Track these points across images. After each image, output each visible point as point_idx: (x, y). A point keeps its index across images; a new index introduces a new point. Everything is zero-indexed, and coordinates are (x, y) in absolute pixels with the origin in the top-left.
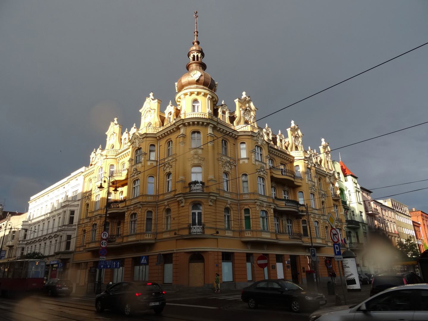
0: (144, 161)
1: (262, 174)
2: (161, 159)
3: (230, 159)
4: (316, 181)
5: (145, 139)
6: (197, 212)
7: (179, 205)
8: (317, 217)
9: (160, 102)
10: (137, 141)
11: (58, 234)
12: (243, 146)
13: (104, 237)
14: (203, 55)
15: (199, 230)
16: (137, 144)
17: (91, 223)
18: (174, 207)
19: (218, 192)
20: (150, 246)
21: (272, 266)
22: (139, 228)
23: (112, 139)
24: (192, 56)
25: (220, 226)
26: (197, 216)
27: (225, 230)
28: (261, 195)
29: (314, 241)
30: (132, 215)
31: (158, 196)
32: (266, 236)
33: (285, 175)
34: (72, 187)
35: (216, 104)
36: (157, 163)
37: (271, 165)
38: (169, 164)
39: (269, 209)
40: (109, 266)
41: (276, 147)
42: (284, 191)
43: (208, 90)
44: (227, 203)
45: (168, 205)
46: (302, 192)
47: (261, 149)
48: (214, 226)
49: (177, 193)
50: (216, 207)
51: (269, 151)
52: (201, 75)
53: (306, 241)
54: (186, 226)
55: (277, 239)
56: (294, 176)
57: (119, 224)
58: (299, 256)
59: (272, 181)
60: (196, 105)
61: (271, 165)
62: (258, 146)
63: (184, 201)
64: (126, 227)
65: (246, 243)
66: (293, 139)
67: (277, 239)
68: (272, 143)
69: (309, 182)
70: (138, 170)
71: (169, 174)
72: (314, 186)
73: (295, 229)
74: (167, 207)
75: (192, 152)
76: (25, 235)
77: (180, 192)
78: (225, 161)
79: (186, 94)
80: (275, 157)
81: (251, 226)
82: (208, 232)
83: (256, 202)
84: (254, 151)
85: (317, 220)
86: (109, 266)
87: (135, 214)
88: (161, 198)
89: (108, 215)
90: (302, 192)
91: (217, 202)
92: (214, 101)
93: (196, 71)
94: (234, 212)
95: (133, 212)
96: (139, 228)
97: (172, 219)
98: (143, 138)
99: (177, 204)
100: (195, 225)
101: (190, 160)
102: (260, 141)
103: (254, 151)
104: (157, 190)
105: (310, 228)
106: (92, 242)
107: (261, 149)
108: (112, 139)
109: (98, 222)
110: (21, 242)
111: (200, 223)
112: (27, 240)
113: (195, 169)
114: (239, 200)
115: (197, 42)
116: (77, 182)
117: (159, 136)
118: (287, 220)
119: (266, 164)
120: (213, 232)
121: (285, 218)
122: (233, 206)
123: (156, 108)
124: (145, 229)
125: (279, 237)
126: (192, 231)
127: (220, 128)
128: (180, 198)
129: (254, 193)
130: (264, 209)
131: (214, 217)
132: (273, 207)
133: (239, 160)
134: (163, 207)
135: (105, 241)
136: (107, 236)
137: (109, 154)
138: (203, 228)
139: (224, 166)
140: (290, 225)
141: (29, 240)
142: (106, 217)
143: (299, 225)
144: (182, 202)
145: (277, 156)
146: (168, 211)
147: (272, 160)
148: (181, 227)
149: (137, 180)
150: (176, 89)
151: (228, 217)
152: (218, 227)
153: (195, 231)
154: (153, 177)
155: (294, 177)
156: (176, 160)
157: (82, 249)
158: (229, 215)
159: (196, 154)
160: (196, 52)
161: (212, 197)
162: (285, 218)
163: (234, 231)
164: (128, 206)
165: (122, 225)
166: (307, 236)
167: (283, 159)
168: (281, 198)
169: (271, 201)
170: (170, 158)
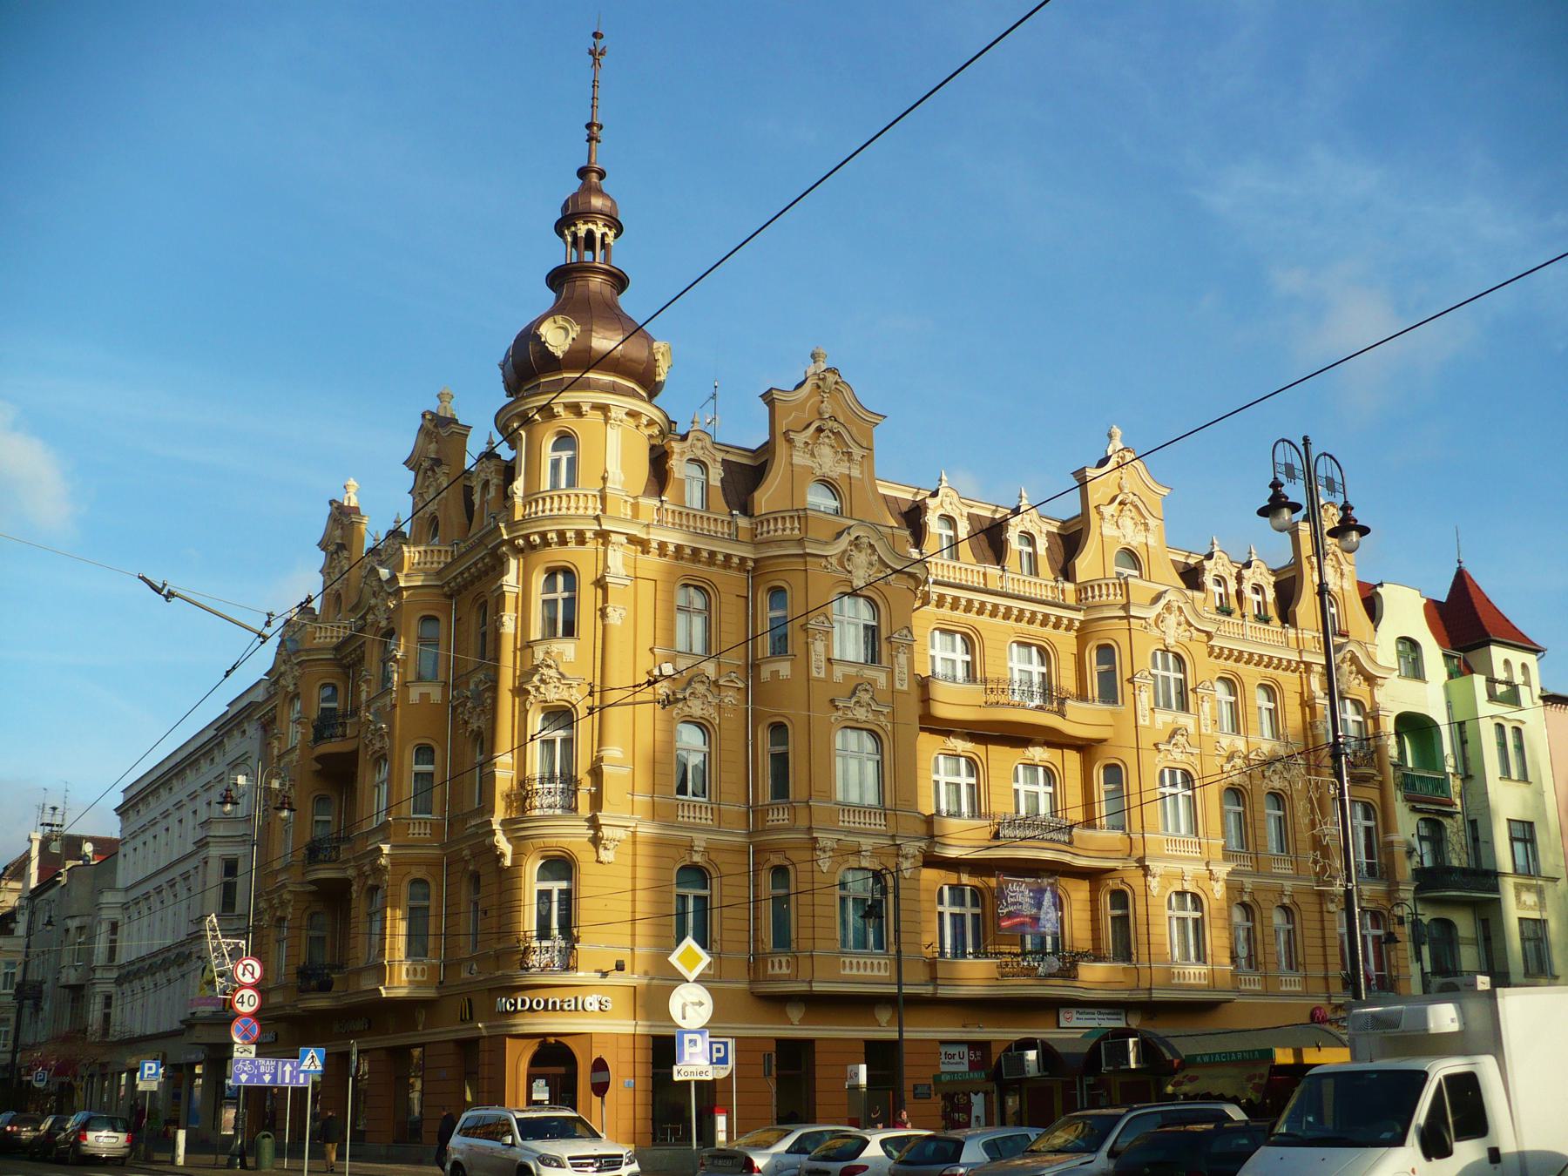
6: (557, 886)
11: (186, 950)
13: (248, 979)
21: (915, 1087)
26: (555, 906)
60: (565, 456)
135: (251, 992)
136: (257, 974)
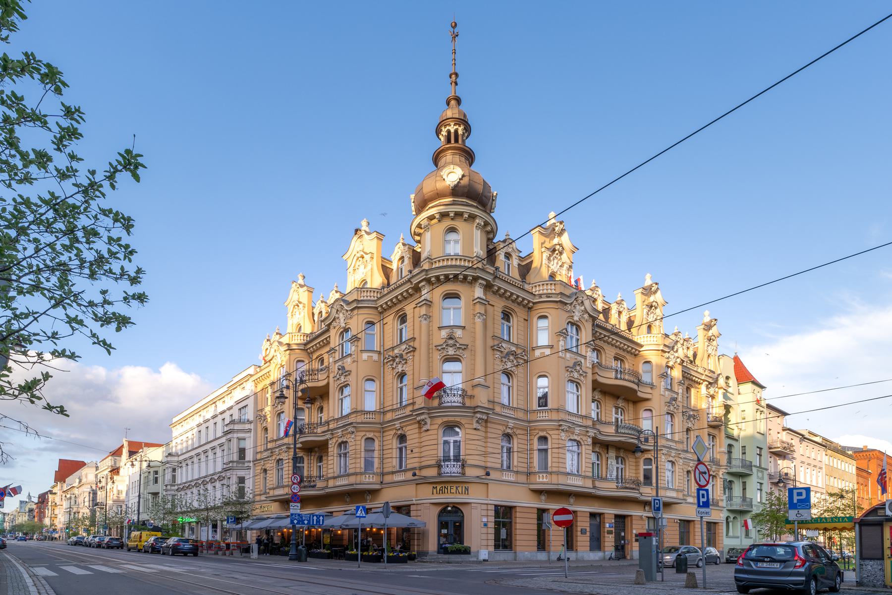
1: (576, 375)
2: (386, 348)
3: (517, 348)
4: (680, 391)
5: (356, 312)
6: (451, 439)
7: (420, 428)
8: (673, 454)
9: (380, 237)
10: (341, 315)
12: (543, 323)
14: (468, 129)
15: (455, 470)
16: (342, 320)
18: (411, 432)
19: (491, 407)
20: (374, 493)
22: (353, 466)
24: (444, 133)
25: (493, 462)
27: (501, 470)
28: (570, 414)
29: (661, 493)
30: (340, 445)
31: (384, 413)
32: (575, 483)
33: (621, 379)
35: (494, 237)
37: (596, 361)
38: (401, 356)
39: (584, 438)
40: (306, 522)
41: (609, 327)
42: (617, 408)
43: (477, 207)
44: (507, 426)
46: (650, 410)
47: (578, 329)
48: (482, 464)
49: (417, 407)
50: (486, 432)
51: (593, 334)
52: (463, 176)
53: (647, 493)
54: (433, 462)
55: (594, 487)
56: (639, 380)
57: (320, 459)
58: (631, 516)
59: (594, 389)
61: (596, 361)
62: (573, 324)
63: (428, 421)
64: (332, 464)
65: (539, 492)
66: (645, 311)
67: (594, 487)
68: (601, 317)
69: (667, 393)
70: (347, 369)
71: (402, 376)
72: (675, 399)
73: (629, 473)
74: (399, 432)
75: (444, 333)
77: (423, 405)
78: (506, 351)
79: (431, 218)
80: (605, 346)
81: (549, 465)
82: (471, 472)
83: (560, 425)
84: (563, 334)
85: (671, 459)
86: (306, 522)
88: (389, 416)
89: (298, 446)
90: (650, 410)
91: (489, 425)
92: (488, 233)
93: (452, 166)
94: (520, 441)
96: (353, 466)
97: (409, 452)
98: (352, 310)
99: (417, 426)
100: (449, 460)
102: (577, 313)
103: (563, 334)
104: (382, 403)
105: (657, 467)
106: (278, 487)
107: (578, 329)
109: (284, 456)
111: (457, 458)
113: (449, 366)
114: (529, 422)
115: (455, 99)
117: (381, 306)
118: (617, 458)
119: (585, 357)
120: (480, 472)
121: (612, 454)
122: (518, 432)
123: (374, 251)
124: (363, 466)
125: (598, 484)
126: (443, 470)
127: (499, 288)
128: (423, 417)
129: (558, 410)
130: (576, 437)
131: (483, 449)
132: (591, 434)
133: (533, 349)
134: (392, 432)
137: (293, 342)
138: (463, 466)
139: (504, 360)
140: (620, 466)
142: (295, 448)
143: (637, 466)
144: (426, 423)
145: (608, 343)
146: (402, 438)
147: (597, 350)
148: (423, 464)
149: (346, 386)
150: (413, 208)
151: (509, 451)
152: (489, 465)
153: (448, 470)
154: (373, 380)
155: (639, 382)
156: (415, 349)
157: (263, 498)
158: (511, 446)
159: (451, 338)
160: (452, 124)
161: (478, 415)
162: (612, 454)
163: (517, 472)
164: (332, 430)
165: (325, 462)
166: (651, 484)
167: (620, 348)
168: (608, 420)
169: (590, 423)
170: (404, 347)
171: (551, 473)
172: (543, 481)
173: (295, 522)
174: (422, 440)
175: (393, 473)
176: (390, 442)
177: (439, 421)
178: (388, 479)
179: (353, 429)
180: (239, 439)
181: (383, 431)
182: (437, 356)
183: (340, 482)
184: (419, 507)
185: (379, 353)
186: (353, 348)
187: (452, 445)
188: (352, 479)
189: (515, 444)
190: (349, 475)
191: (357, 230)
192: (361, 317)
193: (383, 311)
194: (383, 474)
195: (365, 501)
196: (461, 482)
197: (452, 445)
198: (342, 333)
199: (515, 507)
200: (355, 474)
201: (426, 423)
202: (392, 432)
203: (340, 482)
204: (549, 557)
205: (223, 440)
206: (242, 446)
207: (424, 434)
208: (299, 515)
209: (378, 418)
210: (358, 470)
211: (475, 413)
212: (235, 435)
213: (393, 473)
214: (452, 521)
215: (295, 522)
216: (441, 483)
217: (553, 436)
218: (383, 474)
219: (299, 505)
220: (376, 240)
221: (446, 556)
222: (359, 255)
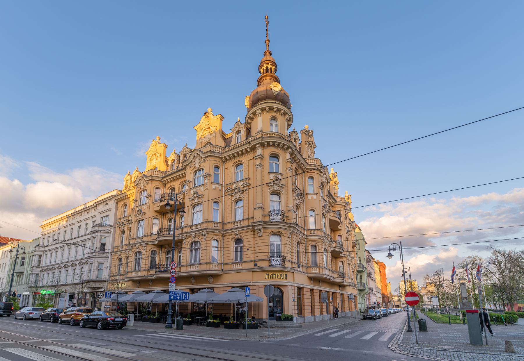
0: (208, 184)
5: (208, 159)
15: (278, 263)
17: (133, 250)
23: (155, 159)
34: (101, 213)
36: (222, 189)
45: (239, 234)
49: (255, 221)
54: (266, 257)
63: (262, 230)
74: (237, 237)
75: (272, 176)
76: (39, 262)
77: (260, 220)
82: (288, 265)
87: (196, 242)
88: (229, 226)
95: (194, 240)
98: (206, 157)
101: (269, 185)
108: (155, 159)
110: (34, 268)
112: (42, 267)
116: (107, 207)
126: (273, 263)
134: (231, 237)
138: (284, 261)
141: (44, 267)
144: (261, 232)
146: (239, 241)
171: (319, 267)
172: (315, 272)
173: (172, 297)
174: (256, 242)
175: (232, 264)
176: (230, 243)
177: (269, 231)
178: (226, 268)
179: (205, 233)
180: (101, 237)
181: (224, 236)
182: (267, 190)
183: (191, 269)
184: (255, 288)
185: (222, 185)
186: (206, 181)
187: (275, 246)
188: (203, 267)
189: (302, 248)
190: (200, 264)
191: (206, 113)
192: (212, 162)
193: (225, 160)
194: (223, 264)
195: (208, 282)
196: (282, 270)
197: (275, 246)
198: (196, 171)
199: (303, 288)
200: (206, 263)
201: (261, 232)
202: (231, 237)
203: (191, 269)
204: (315, 319)
205: (89, 236)
206: (103, 242)
207: (256, 239)
208: (175, 292)
209: (221, 227)
210: (208, 261)
211: (289, 227)
212: (99, 234)
213: (232, 264)
214: (277, 298)
215: (172, 297)
216: (270, 271)
217: (320, 246)
218: (223, 264)
219: (174, 284)
220: (219, 119)
221: (279, 323)
222: (206, 127)
